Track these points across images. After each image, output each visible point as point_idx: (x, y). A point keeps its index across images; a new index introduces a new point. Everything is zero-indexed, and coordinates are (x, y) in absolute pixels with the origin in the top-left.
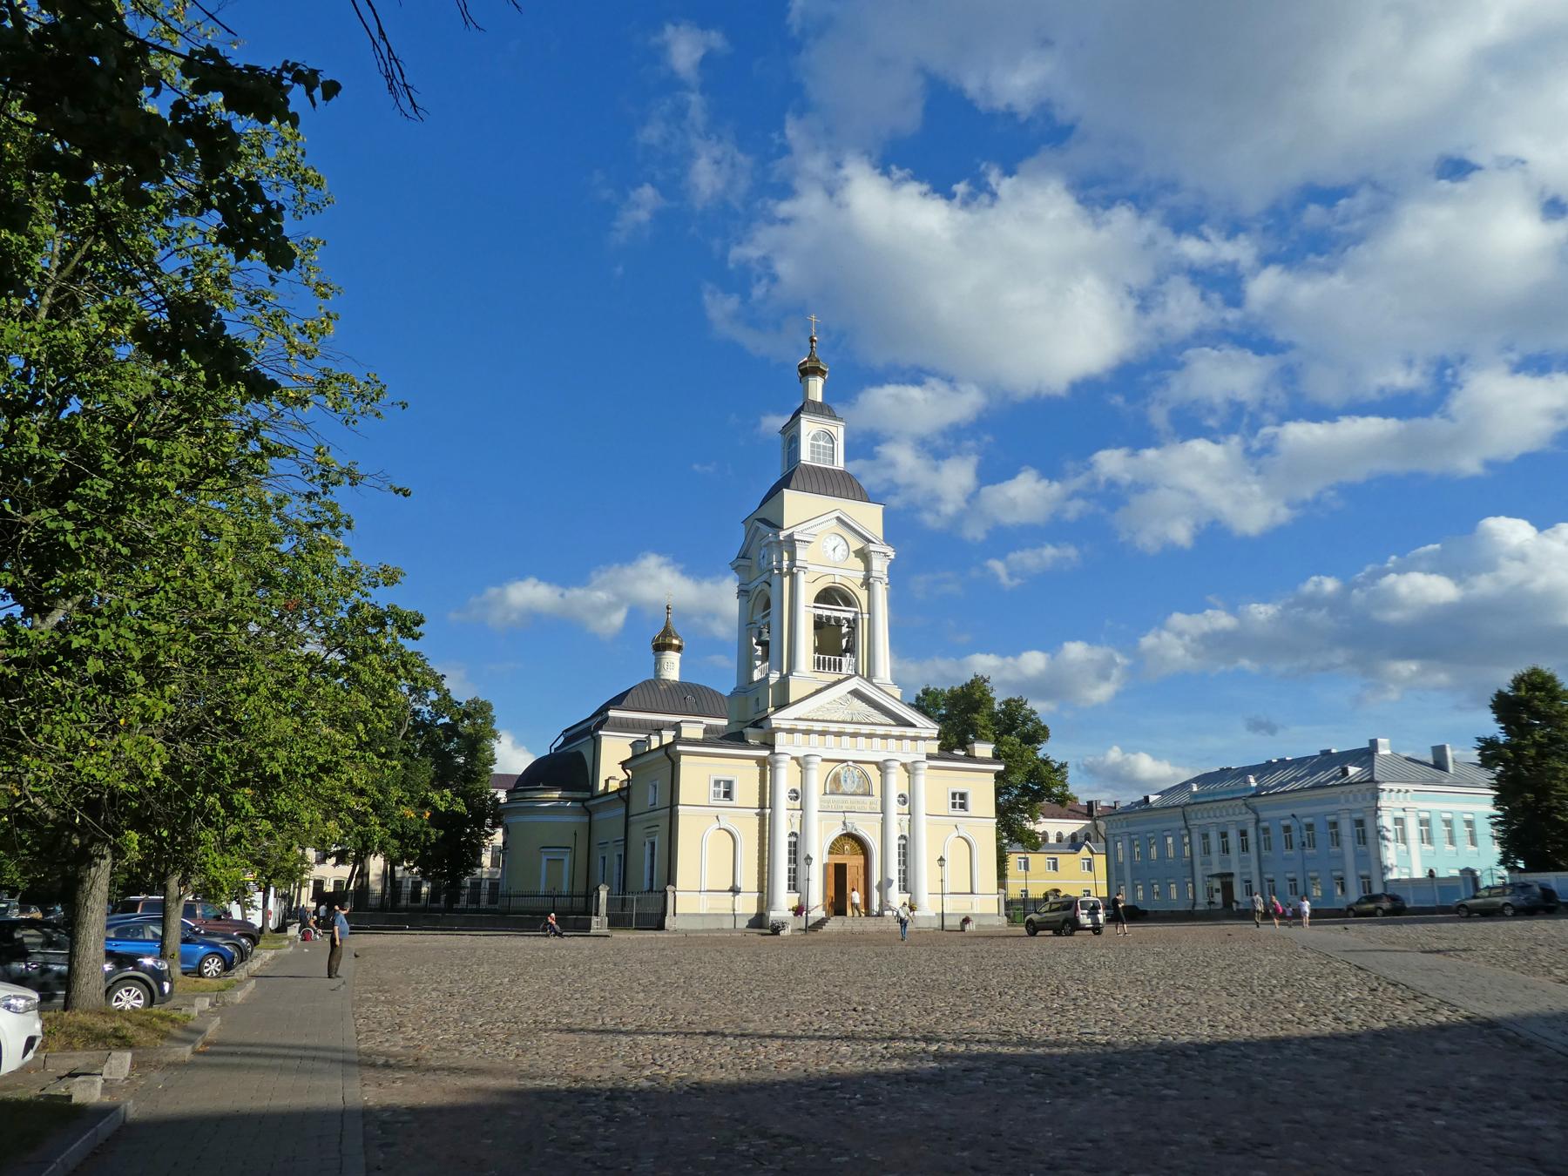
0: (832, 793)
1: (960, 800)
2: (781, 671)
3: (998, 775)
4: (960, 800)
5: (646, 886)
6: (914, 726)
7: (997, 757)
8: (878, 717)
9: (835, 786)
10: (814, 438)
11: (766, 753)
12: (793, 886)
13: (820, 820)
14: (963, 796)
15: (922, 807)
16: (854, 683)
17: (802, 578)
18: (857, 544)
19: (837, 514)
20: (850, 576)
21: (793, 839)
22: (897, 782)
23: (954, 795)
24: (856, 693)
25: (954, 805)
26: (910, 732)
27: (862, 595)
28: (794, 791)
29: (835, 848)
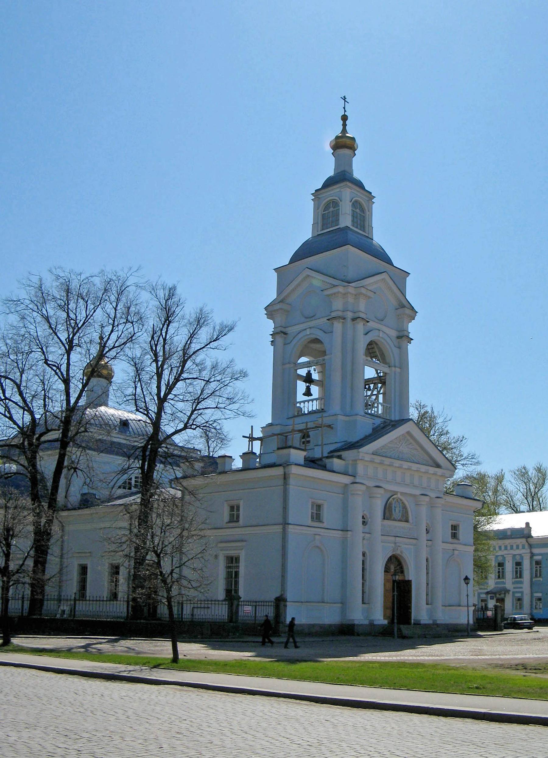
9: (387, 514)
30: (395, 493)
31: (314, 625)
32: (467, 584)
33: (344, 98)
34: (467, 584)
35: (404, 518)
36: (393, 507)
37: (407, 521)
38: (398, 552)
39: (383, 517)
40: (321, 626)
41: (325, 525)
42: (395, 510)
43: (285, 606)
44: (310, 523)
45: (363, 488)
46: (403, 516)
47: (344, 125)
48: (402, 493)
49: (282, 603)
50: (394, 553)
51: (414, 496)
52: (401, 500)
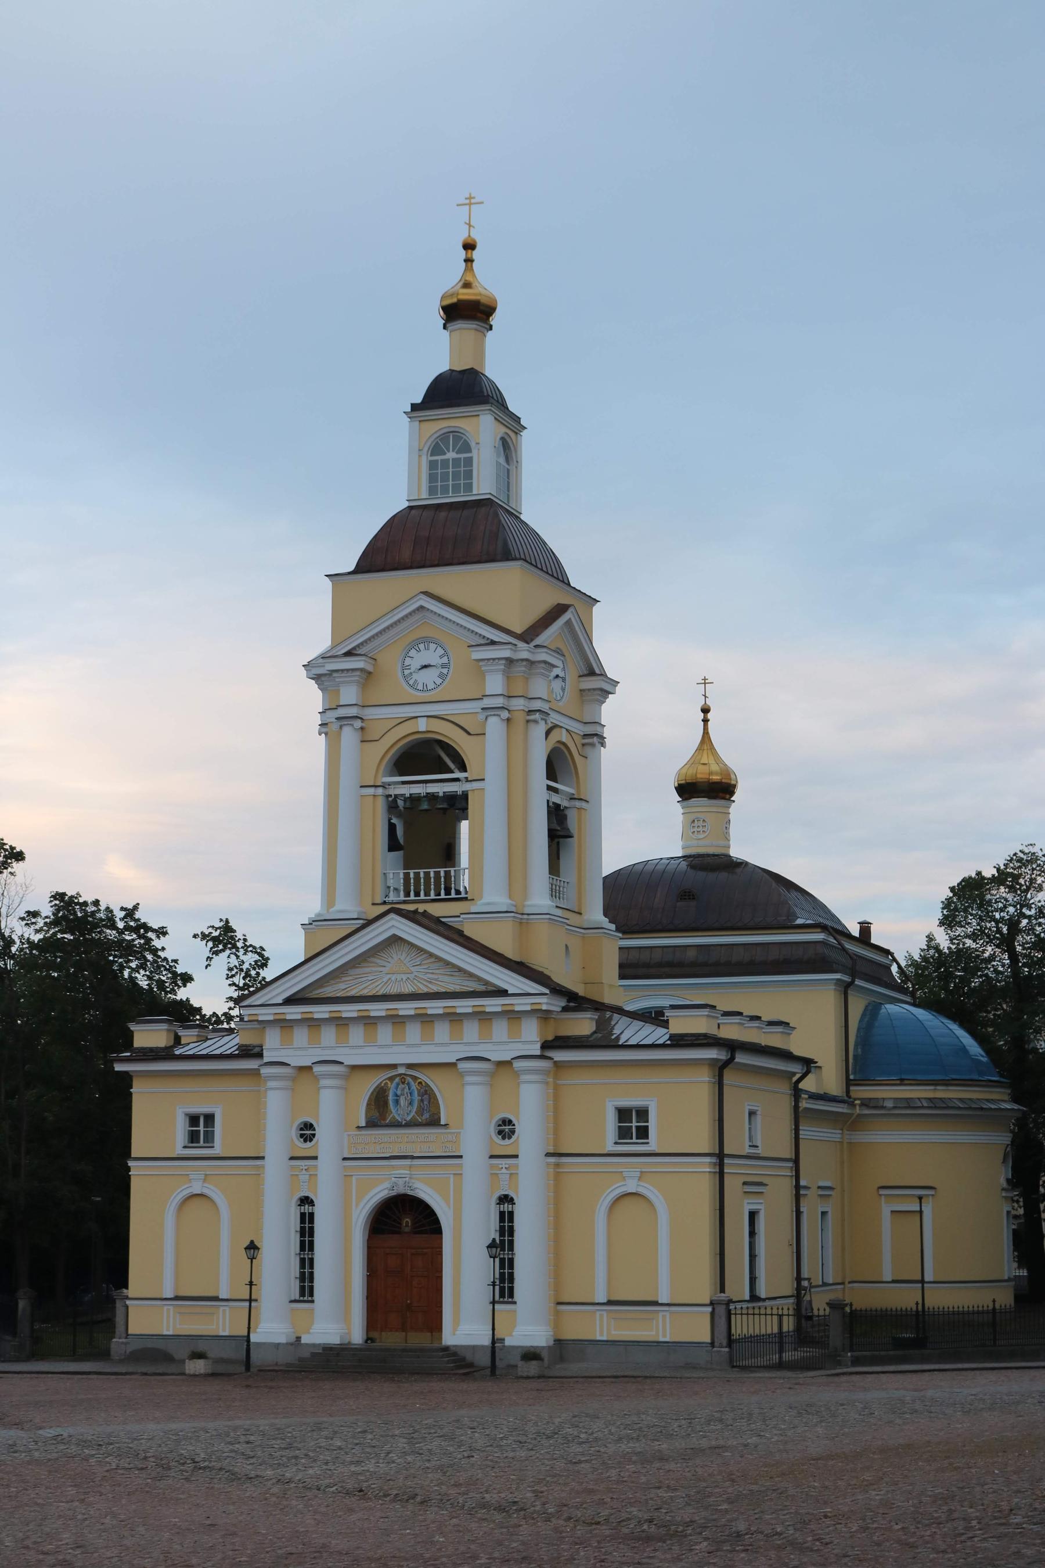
0: (371, 1124)
1: (632, 1123)
6: (503, 993)
9: (378, 1112)
23: (623, 1114)
24: (395, 940)
26: (493, 1005)
28: (308, 1126)
30: (394, 1066)
33: (470, 201)
35: (426, 1116)
36: (391, 1098)
37: (434, 1122)
38: (401, 1190)
41: (218, 1150)
42: (397, 1102)
43: (127, 1307)
44: (180, 1151)
46: (420, 1111)
47: (469, 261)
48: (410, 1066)
50: (394, 1193)
51: (452, 1065)
52: (415, 1078)
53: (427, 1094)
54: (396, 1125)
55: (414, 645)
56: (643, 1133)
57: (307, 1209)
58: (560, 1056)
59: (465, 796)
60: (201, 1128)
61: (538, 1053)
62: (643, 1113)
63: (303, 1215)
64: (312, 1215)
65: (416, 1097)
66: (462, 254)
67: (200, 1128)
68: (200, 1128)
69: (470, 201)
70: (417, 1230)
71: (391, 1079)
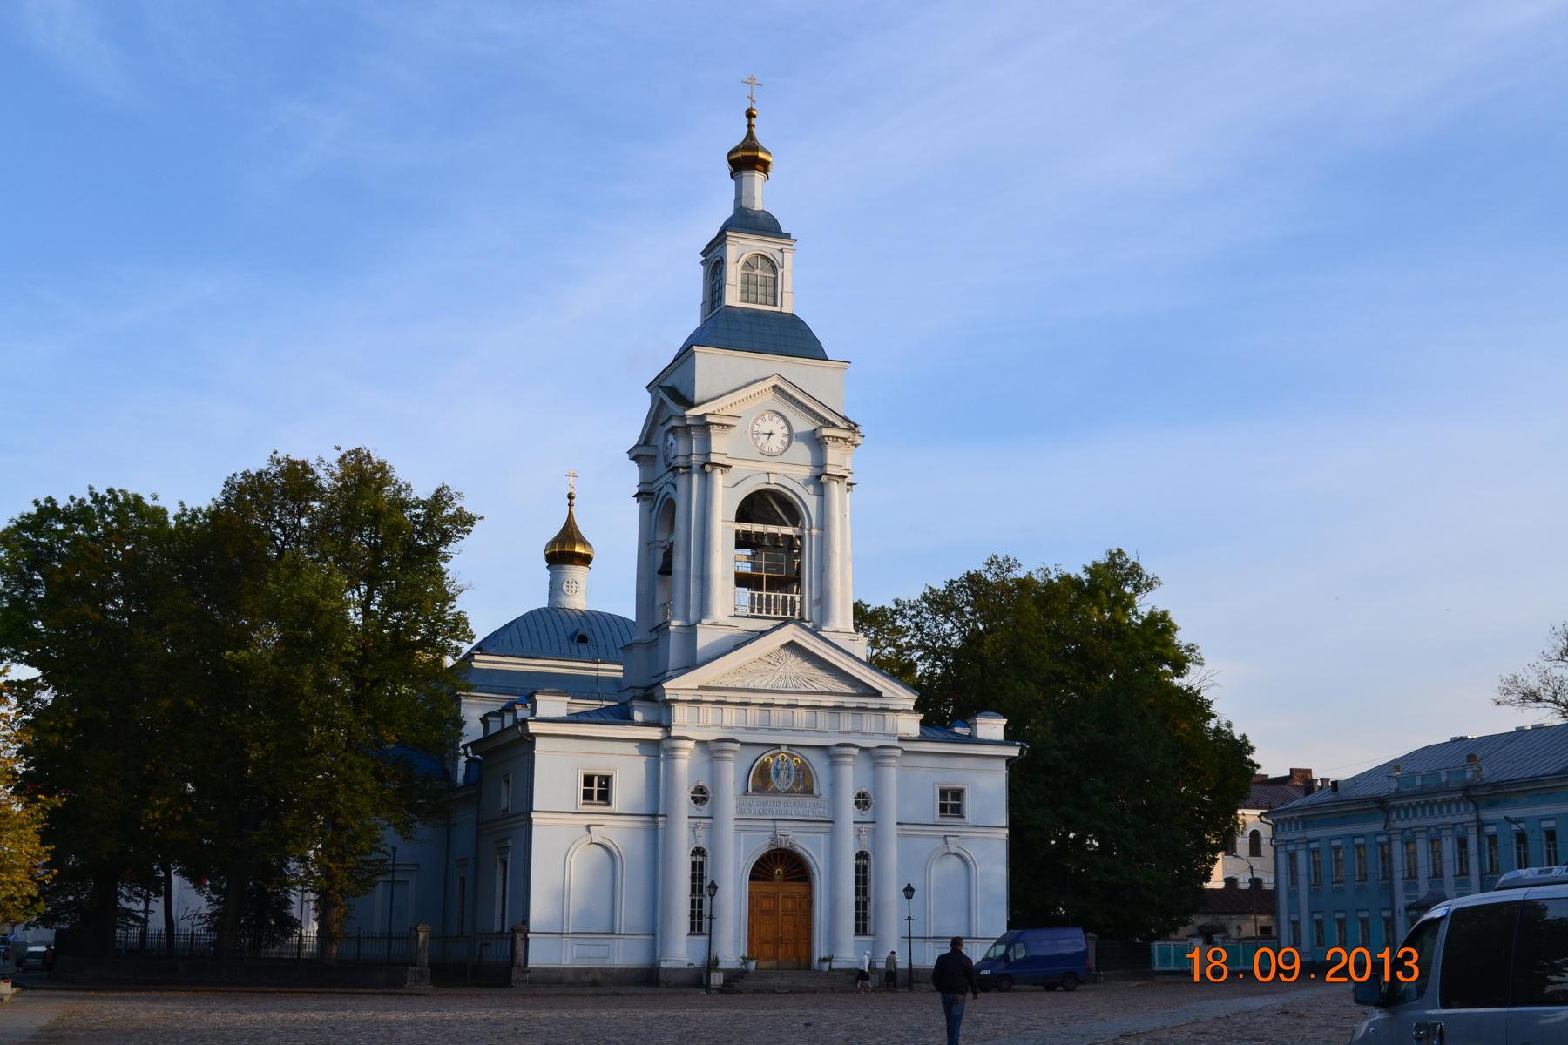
0: (756, 790)
2: (686, 616)
3: (1010, 761)
4: (952, 802)
5: (497, 928)
6: (878, 694)
7: (1010, 736)
8: (826, 682)
9: (761, 780)
10: (748, 265)
11: (655, 734)
12: (696, 927)
13: (738, 830)
14: (958, 794)
15: (892, 808)
16: (790, 633)
17: (719, 478)
18: (803, 424)
19: (774, 381)
20: (791, 474)
21: (698, 859)
22: (852, 778)
23: (943, 793)
24: (792, 646)
25: (943, 808)
26: (872, 702)
27: (810, 501)
28: (700, 790)
29: (761, 871)
30: (778, 746)
31: (587, 971)
32: (909, 898)
33: (751, 82)
34: (909, 898)
37: (809, 791)
38: (783, 845)
39: (741, 789)
40: (606, 972)
42: (777, 775)
43: (527, 940)
45: (692, 744)
46: (797, 783)
47: (750, 126)
48: (789, 746)
49: (519, 937)
53: (804, 772)
54: (776, 792)
55: (761, 417)
56: (958, 811)
57: (698, 859)
58: (908, 746)
59: (800, 537)
60: (596, 788)
61: (896, 744)
62: (958, 794)
63: (694, 864)
64: (701, 864)
65: (793, 772)
66: (746, 121)
67: (597, 789)
68: (597, 789)
69: (751, 82)
70: (788, 878)
71: (773, 756)
